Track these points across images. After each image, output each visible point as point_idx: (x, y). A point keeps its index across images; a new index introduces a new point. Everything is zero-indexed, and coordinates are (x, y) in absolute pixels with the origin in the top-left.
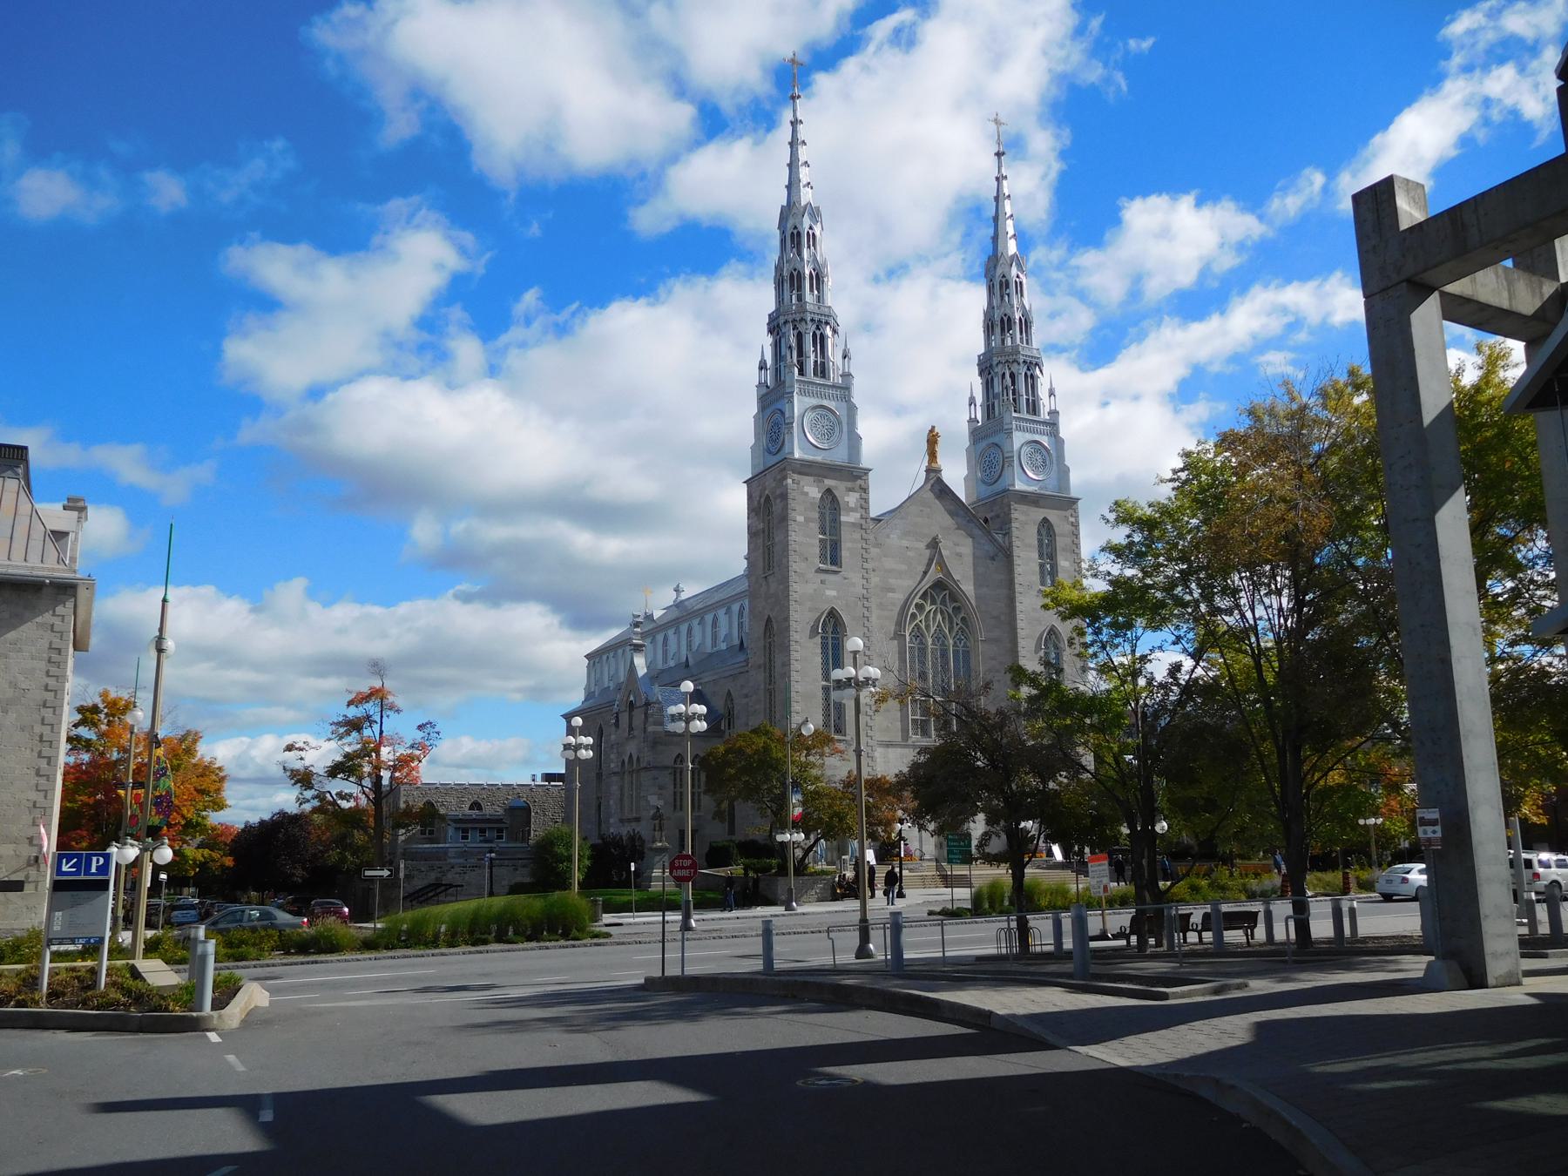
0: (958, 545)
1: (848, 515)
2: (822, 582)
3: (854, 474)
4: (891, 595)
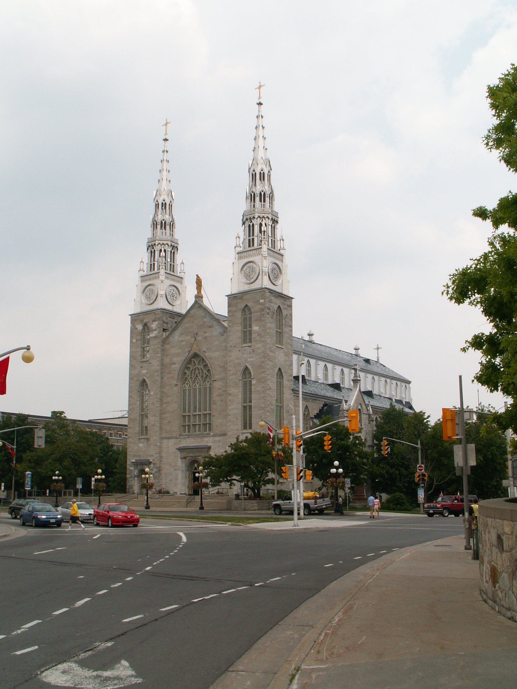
0: (205, 333)
1: (152, 333)
2: (141, 367)
3: (156, 313)
4: (173, 366)
